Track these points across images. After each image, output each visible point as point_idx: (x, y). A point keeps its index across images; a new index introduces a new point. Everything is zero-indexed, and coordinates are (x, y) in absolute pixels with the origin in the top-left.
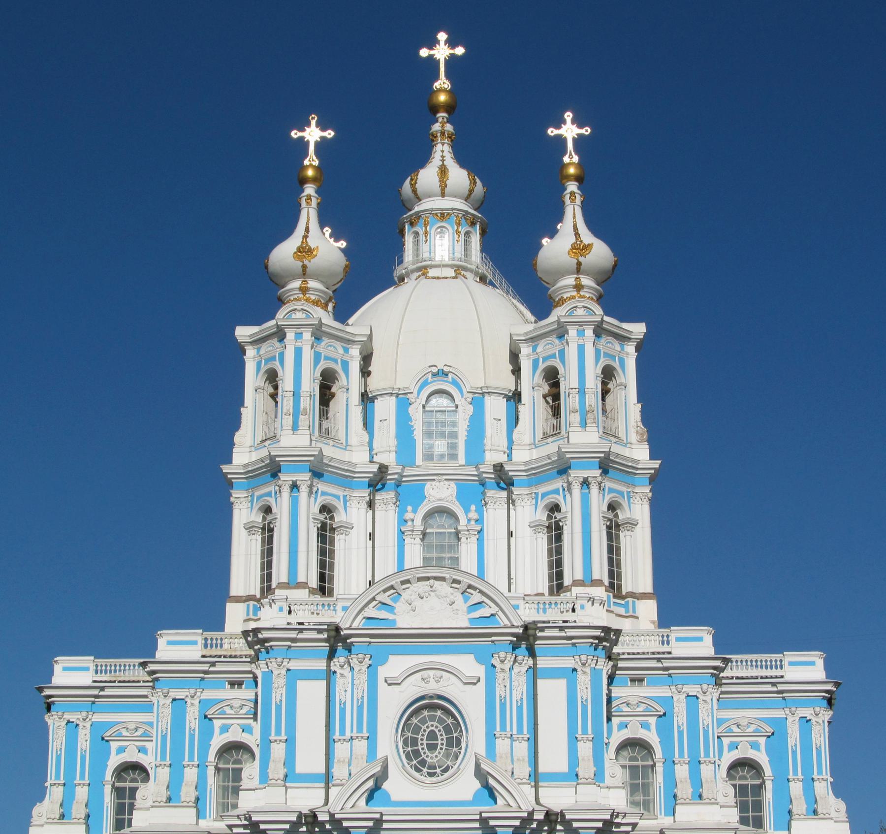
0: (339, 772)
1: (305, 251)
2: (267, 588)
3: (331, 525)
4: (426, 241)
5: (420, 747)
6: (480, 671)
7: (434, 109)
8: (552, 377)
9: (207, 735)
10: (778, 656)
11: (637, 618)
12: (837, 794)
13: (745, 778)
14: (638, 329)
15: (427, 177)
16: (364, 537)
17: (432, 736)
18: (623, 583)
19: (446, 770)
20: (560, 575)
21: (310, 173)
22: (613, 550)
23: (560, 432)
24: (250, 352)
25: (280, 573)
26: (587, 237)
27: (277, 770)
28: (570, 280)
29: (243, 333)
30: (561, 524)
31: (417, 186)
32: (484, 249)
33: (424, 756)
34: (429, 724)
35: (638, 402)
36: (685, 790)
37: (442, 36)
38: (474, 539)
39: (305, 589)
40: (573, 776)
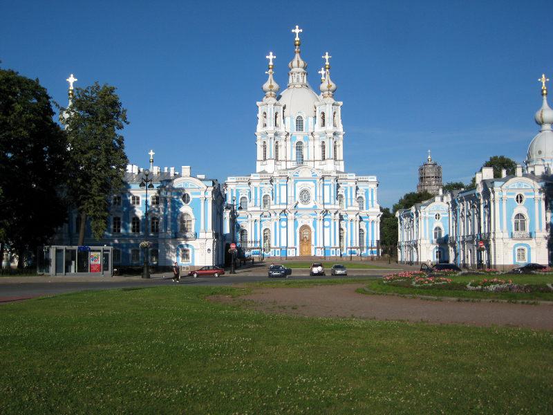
0: (289, 203)
1: (271, 86)
2: (265, 159)
6: (314, 184)
7: (296, 45)
8: (323, 113)
9: (261, 194)
14: (341, 103)
15: (295, 63)
21: (271, 67)
24: (260, 108)
25: (268, 157)
26: (331, 83)
27: (278, 203)
28: (327, 92)
29: (258, 103)
36: (349, 204)
37: (297, 27)
40: (330, 204)
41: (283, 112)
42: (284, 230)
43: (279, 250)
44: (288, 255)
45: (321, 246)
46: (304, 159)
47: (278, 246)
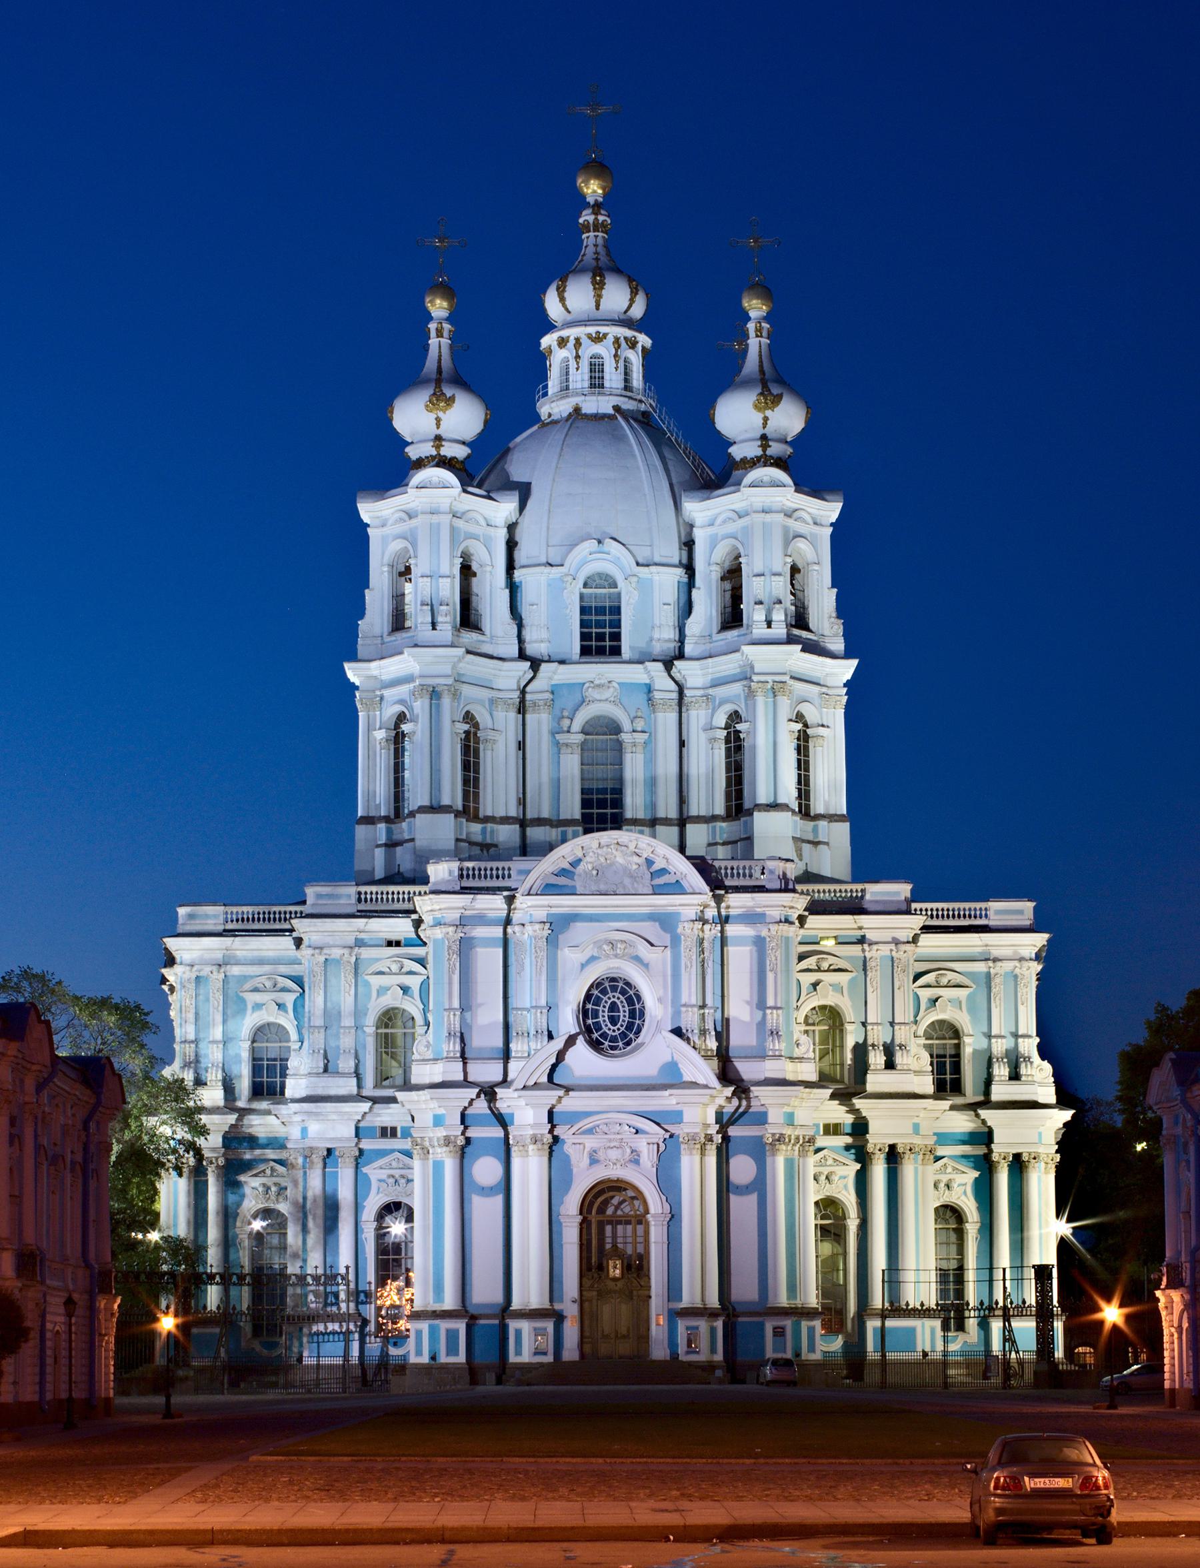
3: (475, 734)
4: (577, 369)
5: (601, 1019)
10: (983, 905)
11: (827, 844)
12: (1043, 1059)
13: (944, 1038)
16: (513, 746)
17: (613, 1007)
18: (812, 803)
19: (628, 1043)
20: (739, 794)
22: (803, 765)
23: (742, 625)
25: (417, 795)
30: (742, 736)
31: (566, 295)
32: (646, 378)
33: (605, 1029)
34: (610, 995)
35: (833, 586)
38: (640, 749)
39: (450, 812)
41: (511, 545)
42: (486, 1210)
43: (461, 1326)
44: (513, 1358)
45: (713, 1301)
46: (629, 814)
47: (449, 1302)
